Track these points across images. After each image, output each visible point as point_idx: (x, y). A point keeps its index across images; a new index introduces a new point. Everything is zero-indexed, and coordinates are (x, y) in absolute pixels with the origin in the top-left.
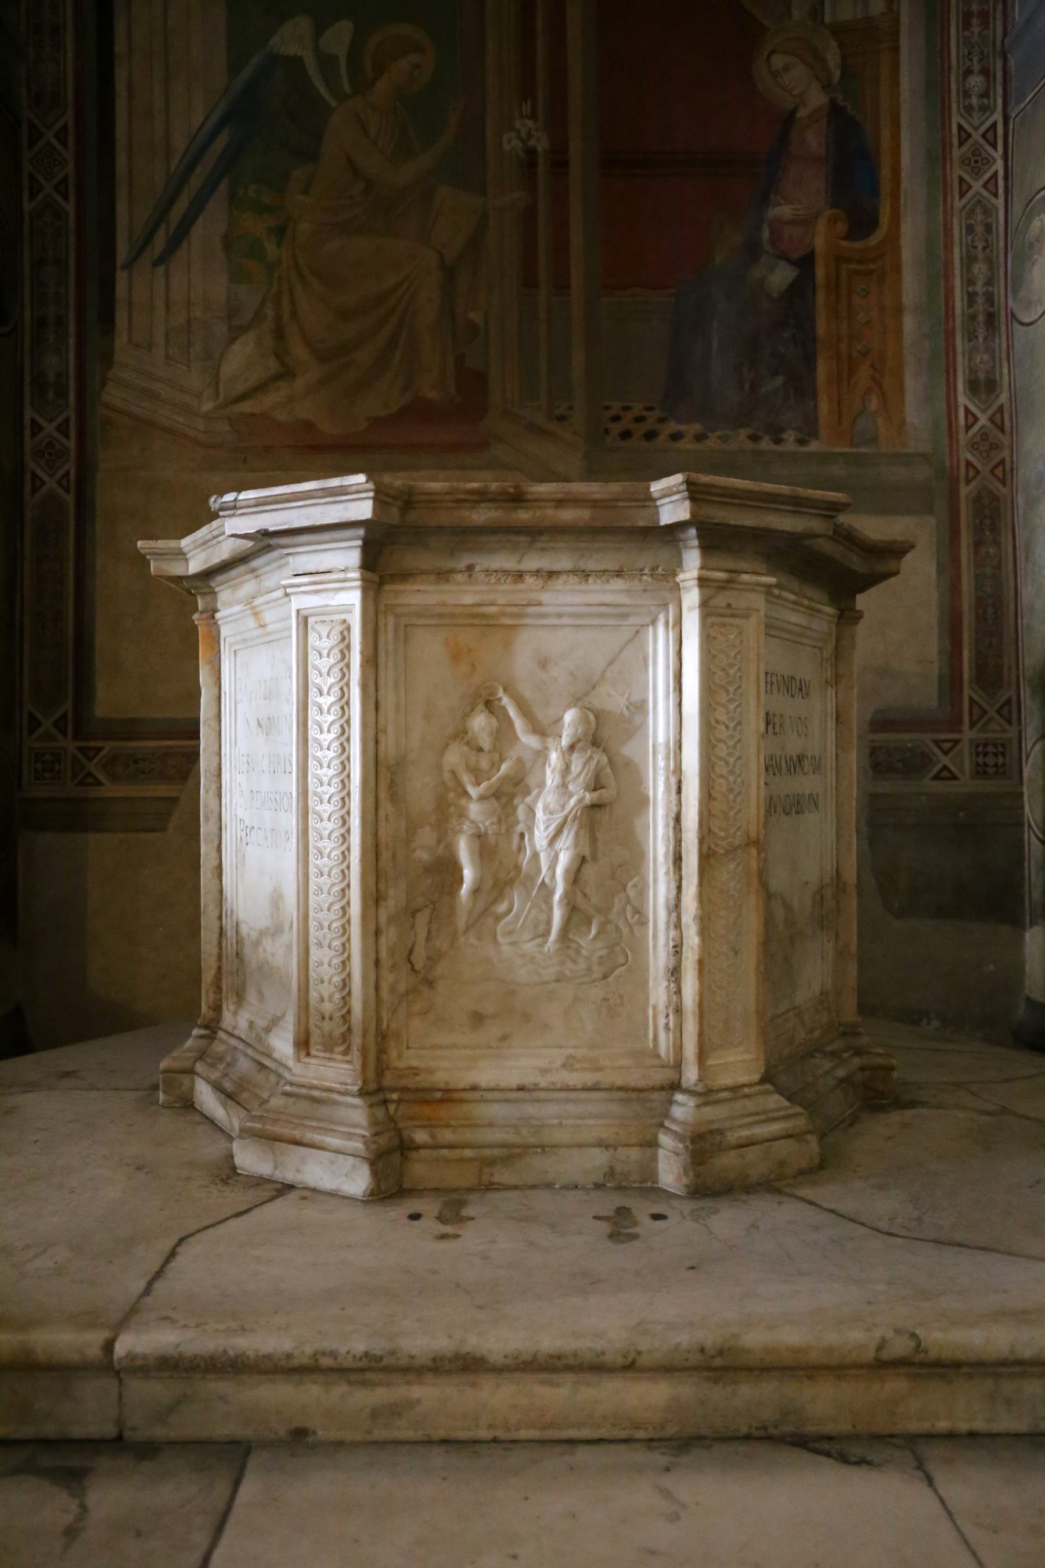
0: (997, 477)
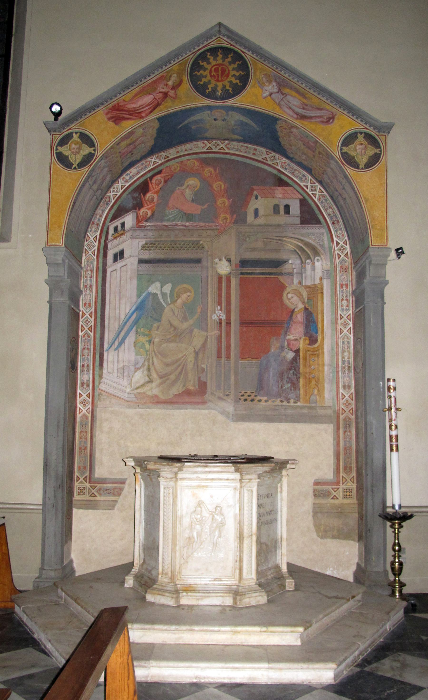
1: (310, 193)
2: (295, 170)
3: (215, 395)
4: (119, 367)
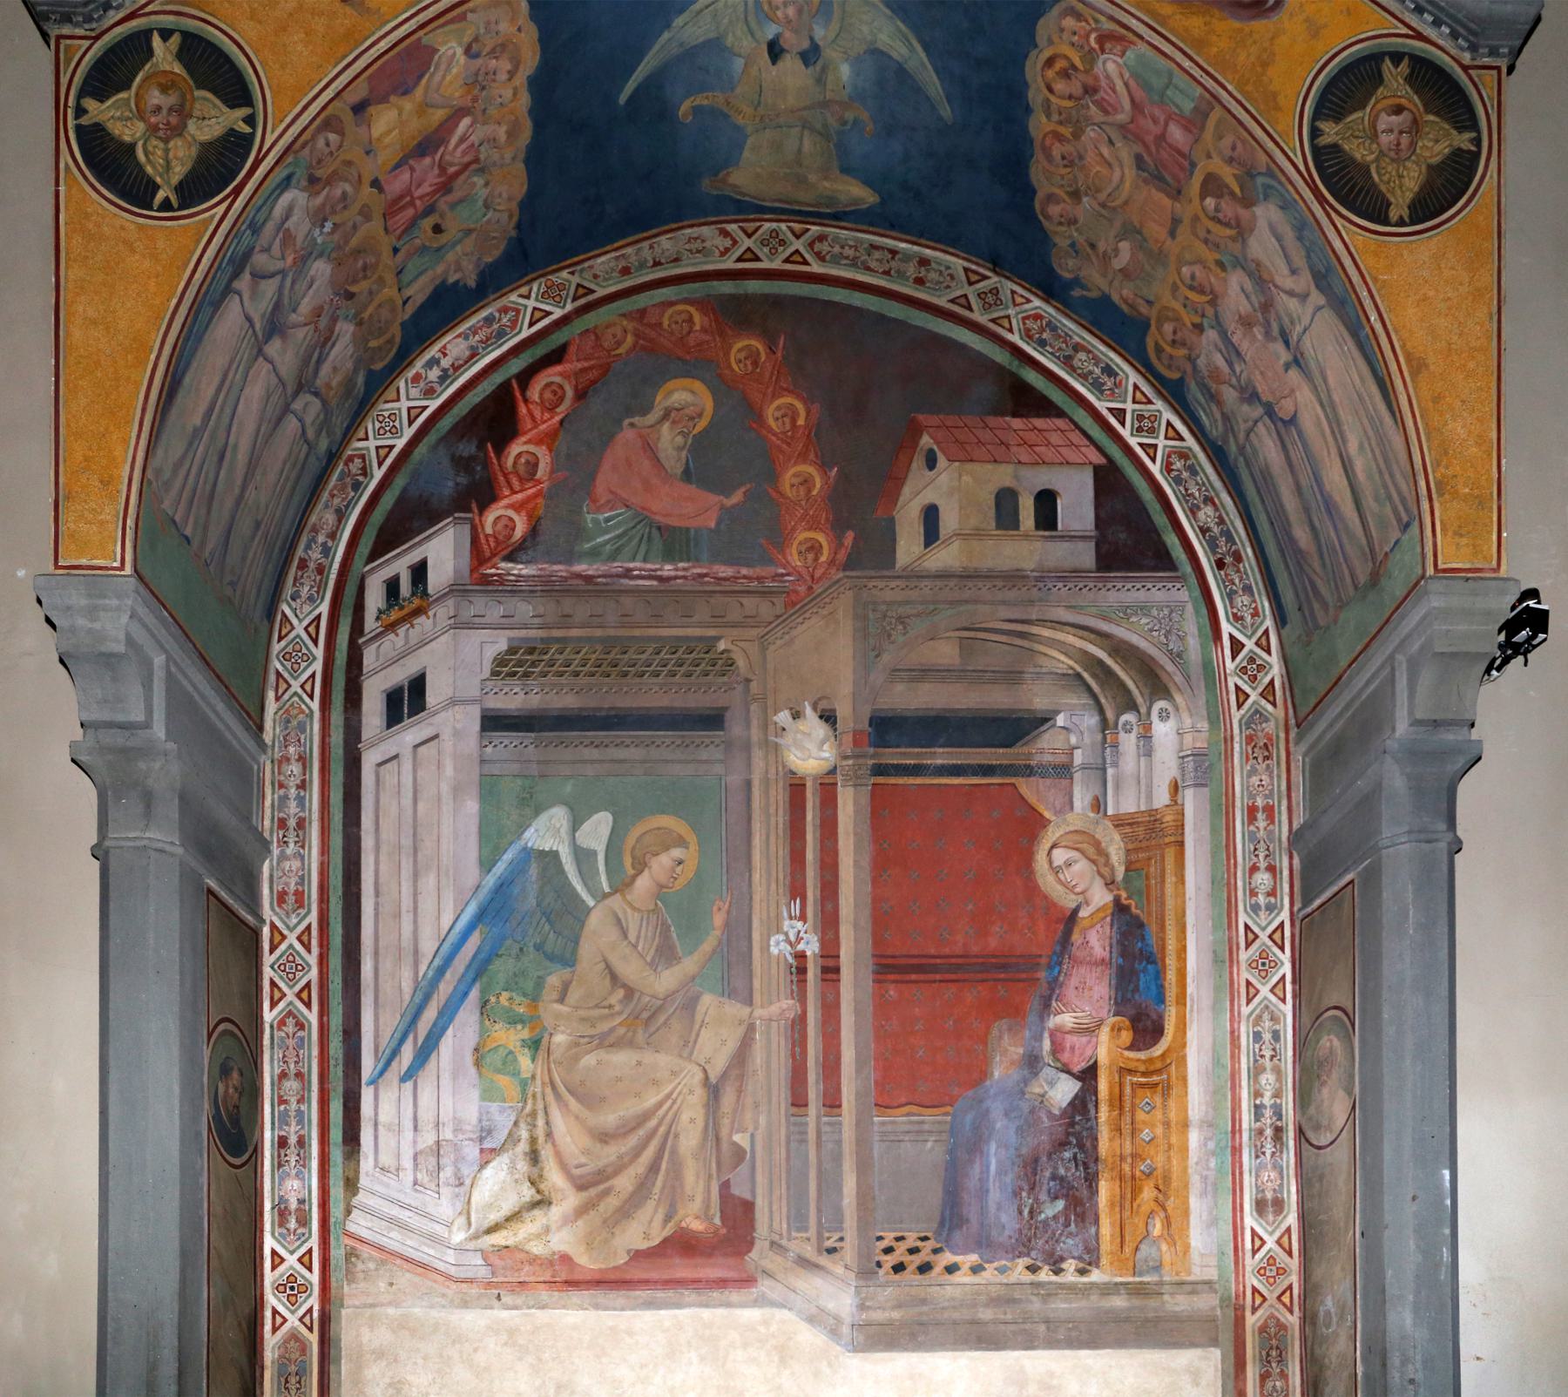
0: (1284, 1305)
1: (1133, 442)
2: (1077, 348)
3: (787, 1250)
4: (421, 1146)
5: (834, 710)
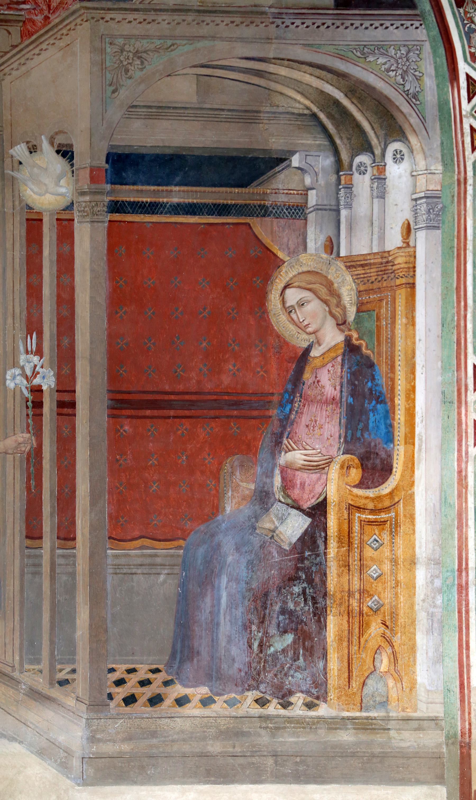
5: (71, 146)
